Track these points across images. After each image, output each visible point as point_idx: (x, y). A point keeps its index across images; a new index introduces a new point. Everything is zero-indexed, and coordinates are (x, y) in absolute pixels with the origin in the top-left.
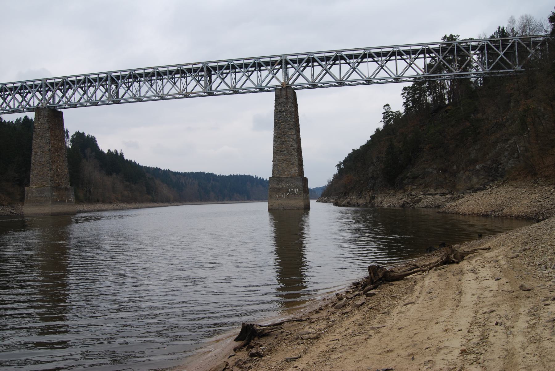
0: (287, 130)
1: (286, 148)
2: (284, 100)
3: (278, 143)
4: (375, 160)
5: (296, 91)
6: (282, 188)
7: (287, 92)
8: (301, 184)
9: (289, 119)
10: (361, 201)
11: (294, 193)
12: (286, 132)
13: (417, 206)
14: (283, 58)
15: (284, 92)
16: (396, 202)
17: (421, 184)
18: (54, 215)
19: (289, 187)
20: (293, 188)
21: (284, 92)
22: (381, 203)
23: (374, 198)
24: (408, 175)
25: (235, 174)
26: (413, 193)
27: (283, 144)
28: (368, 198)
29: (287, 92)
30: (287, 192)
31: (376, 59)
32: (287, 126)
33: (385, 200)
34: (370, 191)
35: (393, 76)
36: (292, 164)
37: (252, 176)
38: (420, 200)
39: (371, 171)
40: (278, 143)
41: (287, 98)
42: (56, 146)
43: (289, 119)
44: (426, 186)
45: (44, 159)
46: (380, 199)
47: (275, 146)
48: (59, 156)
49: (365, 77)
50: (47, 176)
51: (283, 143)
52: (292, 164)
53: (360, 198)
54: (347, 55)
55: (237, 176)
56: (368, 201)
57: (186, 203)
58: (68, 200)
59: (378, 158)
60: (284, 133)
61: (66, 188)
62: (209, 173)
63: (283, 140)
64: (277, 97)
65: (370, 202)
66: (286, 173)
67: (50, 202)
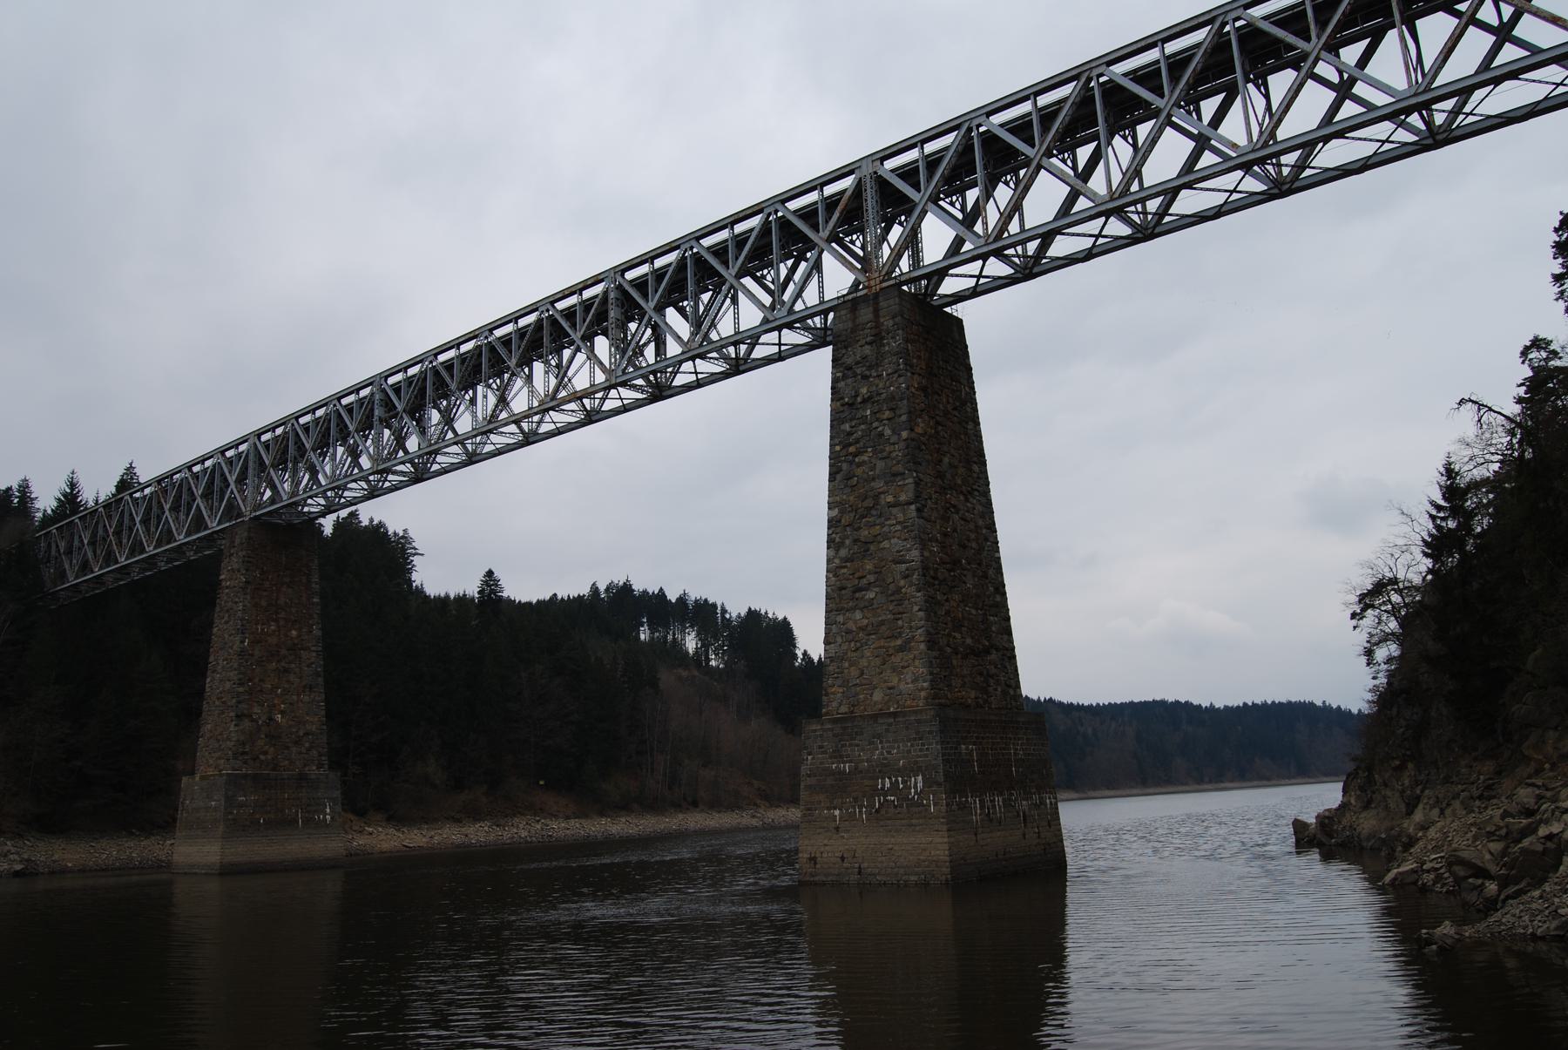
0: (879, 485)
1: (877, 572)
2: (867, 350)
3: (843, 552)
5: (959, 310)
6: (856, 770)
7: (876, 311)
8: (936, 747)
9: (888, 432)
11: (904, 797)
12: (876, 497)
14: (867, 170)
15: (866, 314)
18: (228, 871)
19: (885, 769)
20: (899, 772)
21: (866, 314)
25: (1258, 701)
29: (876, 311)
30: (875, 791)
32: (880, 465)
34: (1401, 768)
35: (1380, 99)
36: (901, 649)
37: (1312, 704)
40: (843, 552)
41: (878, 339)
42: (273, 640)
43: (888, 432)
45: (228, 685)
47: (832, 571)
48: (286, 671)
49: (1234, 146)
50: (229, 739)
51: (864, 548)
52: (901, 649)
53: (1367, 806)
54: (1134, 75)
55: (1265, 704)
58: (307, 821)
60: (869, 503)
61: (302, 777)
62: (1177, 702)
63: (864, 533)
66: (878, 696)
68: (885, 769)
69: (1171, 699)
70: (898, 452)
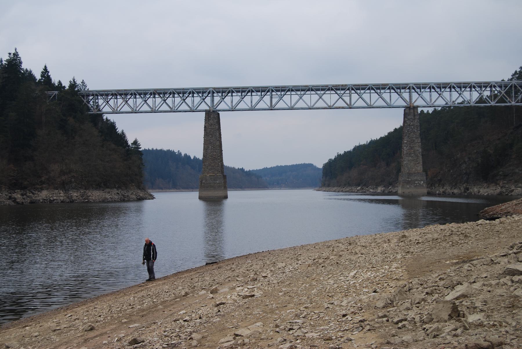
1: (414, 152)
4: (466, 160)
7: (414, 111)
10: (456, 191)
11: (420, 184)
12: (414, 141)
13: (513, 193)
16: (492, 192)
17: (511, 180)
19: (416, 180)
22: (479, 192)
23: (468, 189)
24: (501, 173)
25: (151, 149)
26: (507, 186)
27: (412, 149)
28: (462, 188)
29: (414, 111)
31: (477, 90)
33: (481, 190)
38: (513, 190)
39: (464, 168)
44: (516, 182)
46: (476, 190)
50: (218, 166)
56: (463, 191)
57: (171, 190)
59: (469, 158)
64: (405, 115)
65: (465, 192)
67: (223, 188)
68: (416, 180)
69: (165, 149)
70: (418, 134)
